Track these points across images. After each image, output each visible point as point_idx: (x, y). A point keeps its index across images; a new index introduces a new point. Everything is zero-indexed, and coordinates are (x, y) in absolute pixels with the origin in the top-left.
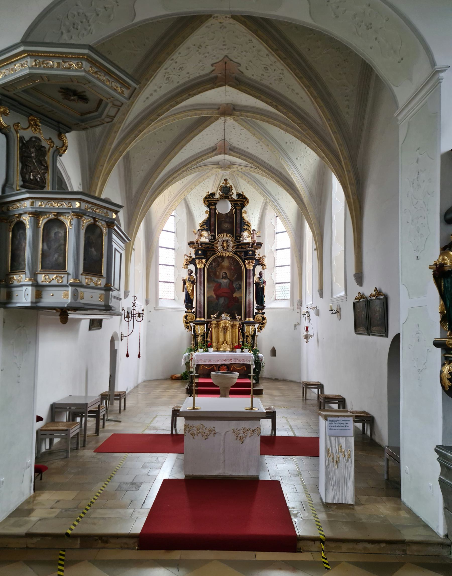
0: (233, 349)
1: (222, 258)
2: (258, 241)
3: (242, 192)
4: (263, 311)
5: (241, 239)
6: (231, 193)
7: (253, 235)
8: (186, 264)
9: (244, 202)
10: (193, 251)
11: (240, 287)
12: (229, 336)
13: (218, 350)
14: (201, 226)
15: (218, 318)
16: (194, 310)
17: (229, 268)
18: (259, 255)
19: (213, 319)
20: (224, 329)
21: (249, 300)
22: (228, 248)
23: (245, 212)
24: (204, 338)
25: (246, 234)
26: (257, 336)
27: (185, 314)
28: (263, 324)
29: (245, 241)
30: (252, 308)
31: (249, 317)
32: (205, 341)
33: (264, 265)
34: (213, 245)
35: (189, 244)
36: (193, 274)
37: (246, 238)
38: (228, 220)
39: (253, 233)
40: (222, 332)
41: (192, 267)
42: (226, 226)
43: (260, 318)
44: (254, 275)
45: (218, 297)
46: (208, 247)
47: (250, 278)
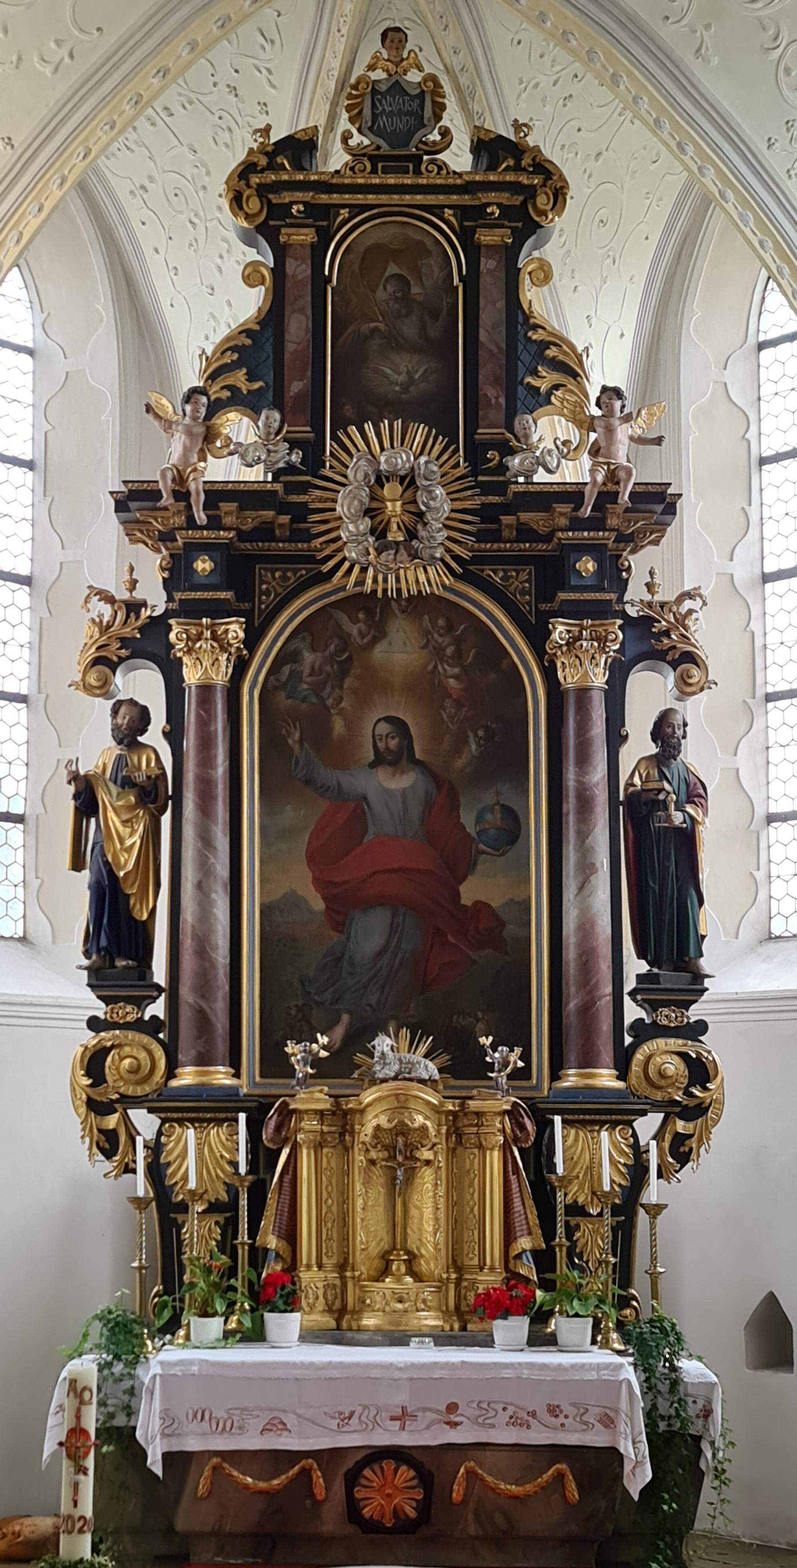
0: (468, 1320)
1: (372, 608)
2: (646, 471)
3: (517, 126)
4: (695, 1013)
5: (515, 462)
6: (435, 136)
7: (610, 431)
8: (97, 661)
9: (530, 192)
11: (512, 831)
12: (428, 1213)
14: (213, 377)
16: (157, 1009)
17: (425, 688)
18: (650, 587)
19: (302, 1070)
20: (391, 1149)
21: (586, 928)
22: (412, 535)
23: (544, 275)
24: (230, 1227)
25: (548, 429)
26: (655, 1210)
27: (89, 1038)
28: (697, 1111)
29: (541, 476)
30: (609, 989)
31: (588, 1061)
32: (243, 1254)
33: (690, 658)
34: (301, 513)
35: (121, 506)
36: (154, 736)
37: (554, 450)
38: (409, 329)
39: (609, 414)
40: (379, 1176)
41: (144, 684)
42: (398, 371)
43: (674, 1067)
44: (616, 737)
45: (342, 905)
46: (265, 532)
47: (584, 759)
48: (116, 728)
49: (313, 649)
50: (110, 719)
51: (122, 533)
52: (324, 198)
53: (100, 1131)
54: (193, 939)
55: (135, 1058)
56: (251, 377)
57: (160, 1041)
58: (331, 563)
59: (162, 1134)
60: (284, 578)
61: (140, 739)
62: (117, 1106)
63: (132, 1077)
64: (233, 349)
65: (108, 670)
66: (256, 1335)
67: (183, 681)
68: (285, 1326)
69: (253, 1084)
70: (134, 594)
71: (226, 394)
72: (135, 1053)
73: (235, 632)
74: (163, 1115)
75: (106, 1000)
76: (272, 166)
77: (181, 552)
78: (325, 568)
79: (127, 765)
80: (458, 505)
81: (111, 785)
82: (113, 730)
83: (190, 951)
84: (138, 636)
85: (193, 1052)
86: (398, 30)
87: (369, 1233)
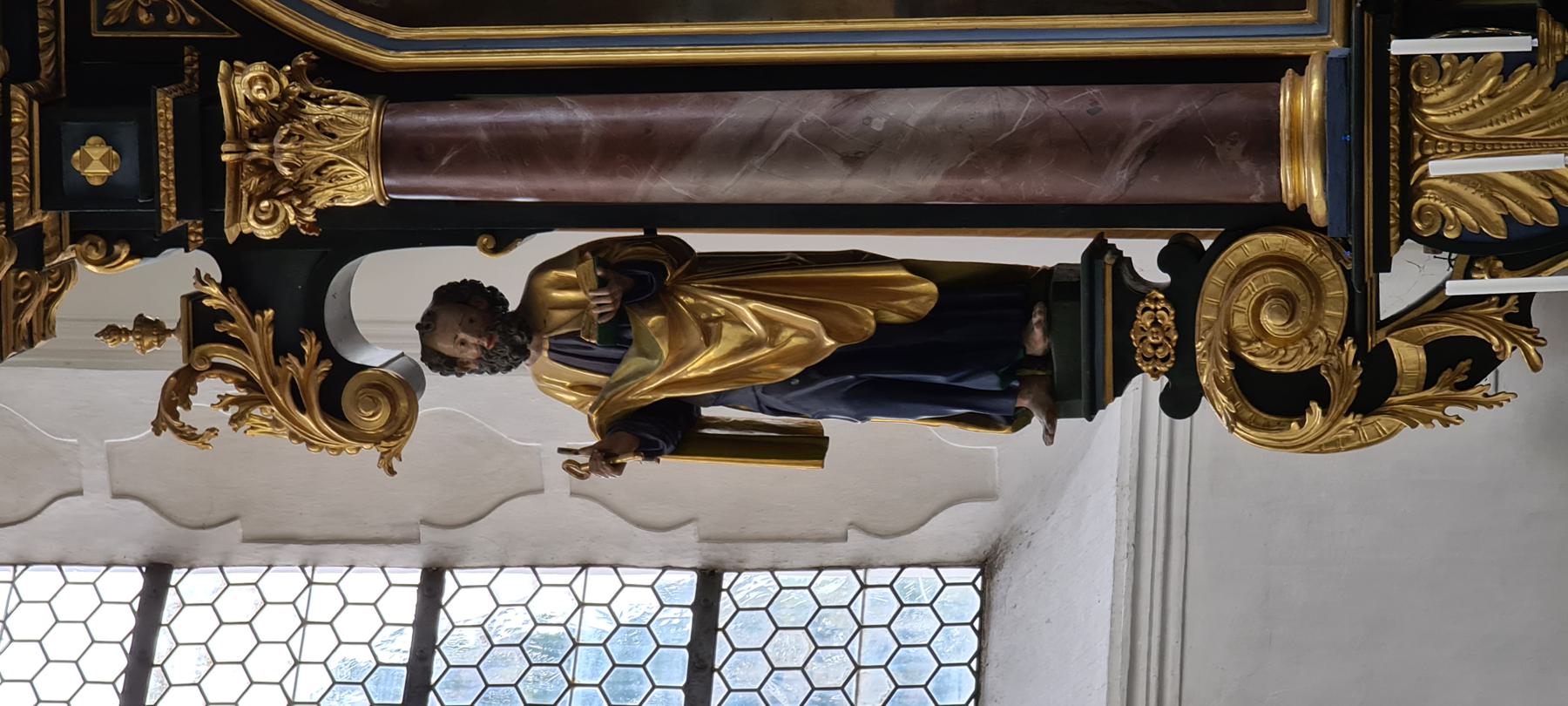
8: (332, 409)
10: (103, 288)
16: (1144, 254)
27: (1210, 416)
36: (507, 273)
41: (385, 299)
48: (492, 363)
50: (467, 377)
51: (27, 356)
53: (1429, 382)
54: (980, 173)
55: (1260, 302)
57: (1221, 245)
59: (1439, 235)
61: (512, 307)
62: (1371, 343)
63: (1304, 309)
65: (353, 384)
67: (372, 205)
69: (1318, 27)
70: (170, 326)
72: (1246, 304)
73: (251, 83)
74: (1394, 235)
75: (1125, 373)
77: (66, 215)
79: (574, 335)
81: (623, 370)
82: (493, 371)
83: (1005, 179)
84: (270, 313)
85: (1245, 167)
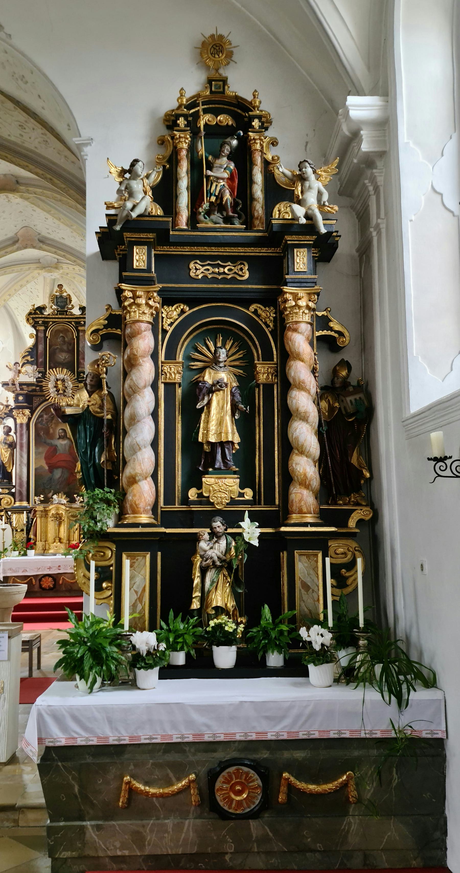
10: (11, 396)
13: (44, 552)
15: (47, 501)
22: (65, 391)
34: (41, 387)
46: (35, 390)
49: (46, 414)
52: (46, 320)
56: (31, 358)
58: (48, 397)
60: (40, 400)
64: (27, 352)
66: (25, 554)
68: (31, 553)
71: (26, 361)
76: (35, 313)
78: (47, 398)
80: (74, 385)
86: (61, 285)
87: (51, 535)
